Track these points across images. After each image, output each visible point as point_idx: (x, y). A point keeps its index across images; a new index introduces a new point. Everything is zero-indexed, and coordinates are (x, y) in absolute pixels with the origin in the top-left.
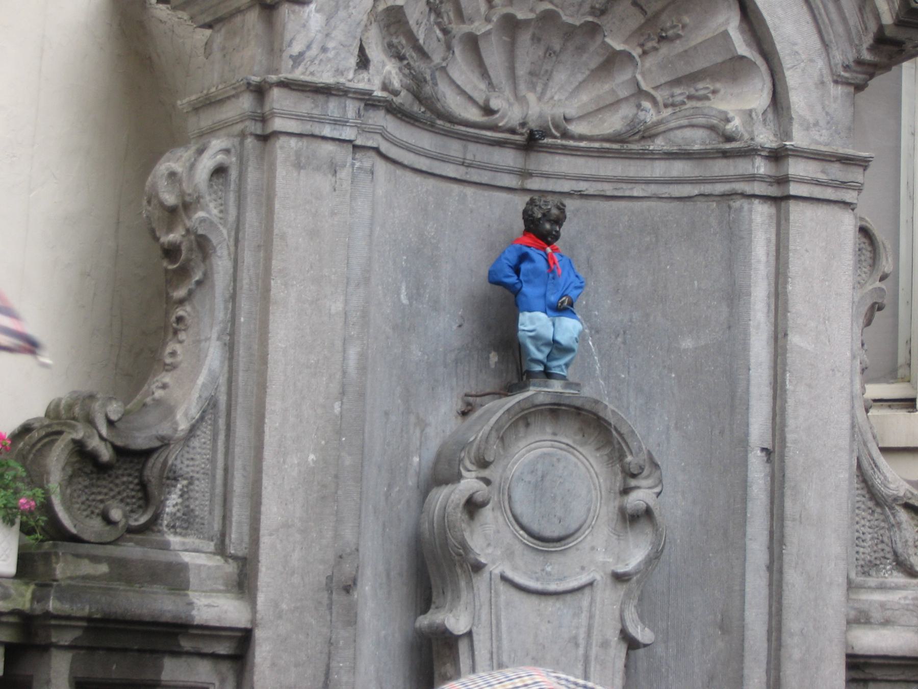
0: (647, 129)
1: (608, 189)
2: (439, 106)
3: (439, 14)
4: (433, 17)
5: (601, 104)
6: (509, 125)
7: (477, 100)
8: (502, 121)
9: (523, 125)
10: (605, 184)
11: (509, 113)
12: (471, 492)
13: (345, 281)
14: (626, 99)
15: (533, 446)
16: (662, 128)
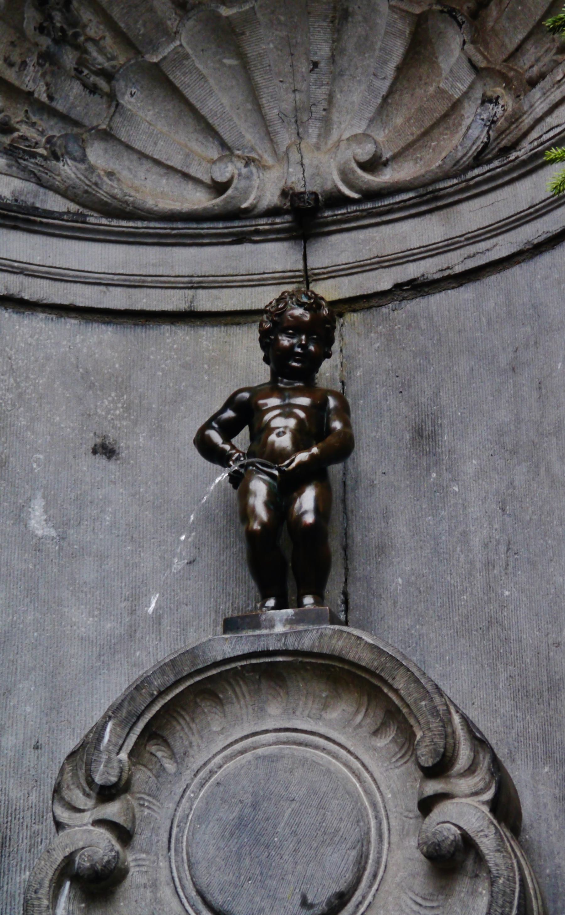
0: (501, 133)
1: (457, 262)
2: (102, 195)
3: (77, 47)
4: (69, 58)
5: (428, 124)
6: (264, 204)
7: (199, 175)
8: (246, 200)
9: (284, 194)
10: (449, 255)
11: (256, 182)
12: (67, 852)
13: (192, 560)
14: (466, 95)
15: (238, 747)
16: (527, 121)
